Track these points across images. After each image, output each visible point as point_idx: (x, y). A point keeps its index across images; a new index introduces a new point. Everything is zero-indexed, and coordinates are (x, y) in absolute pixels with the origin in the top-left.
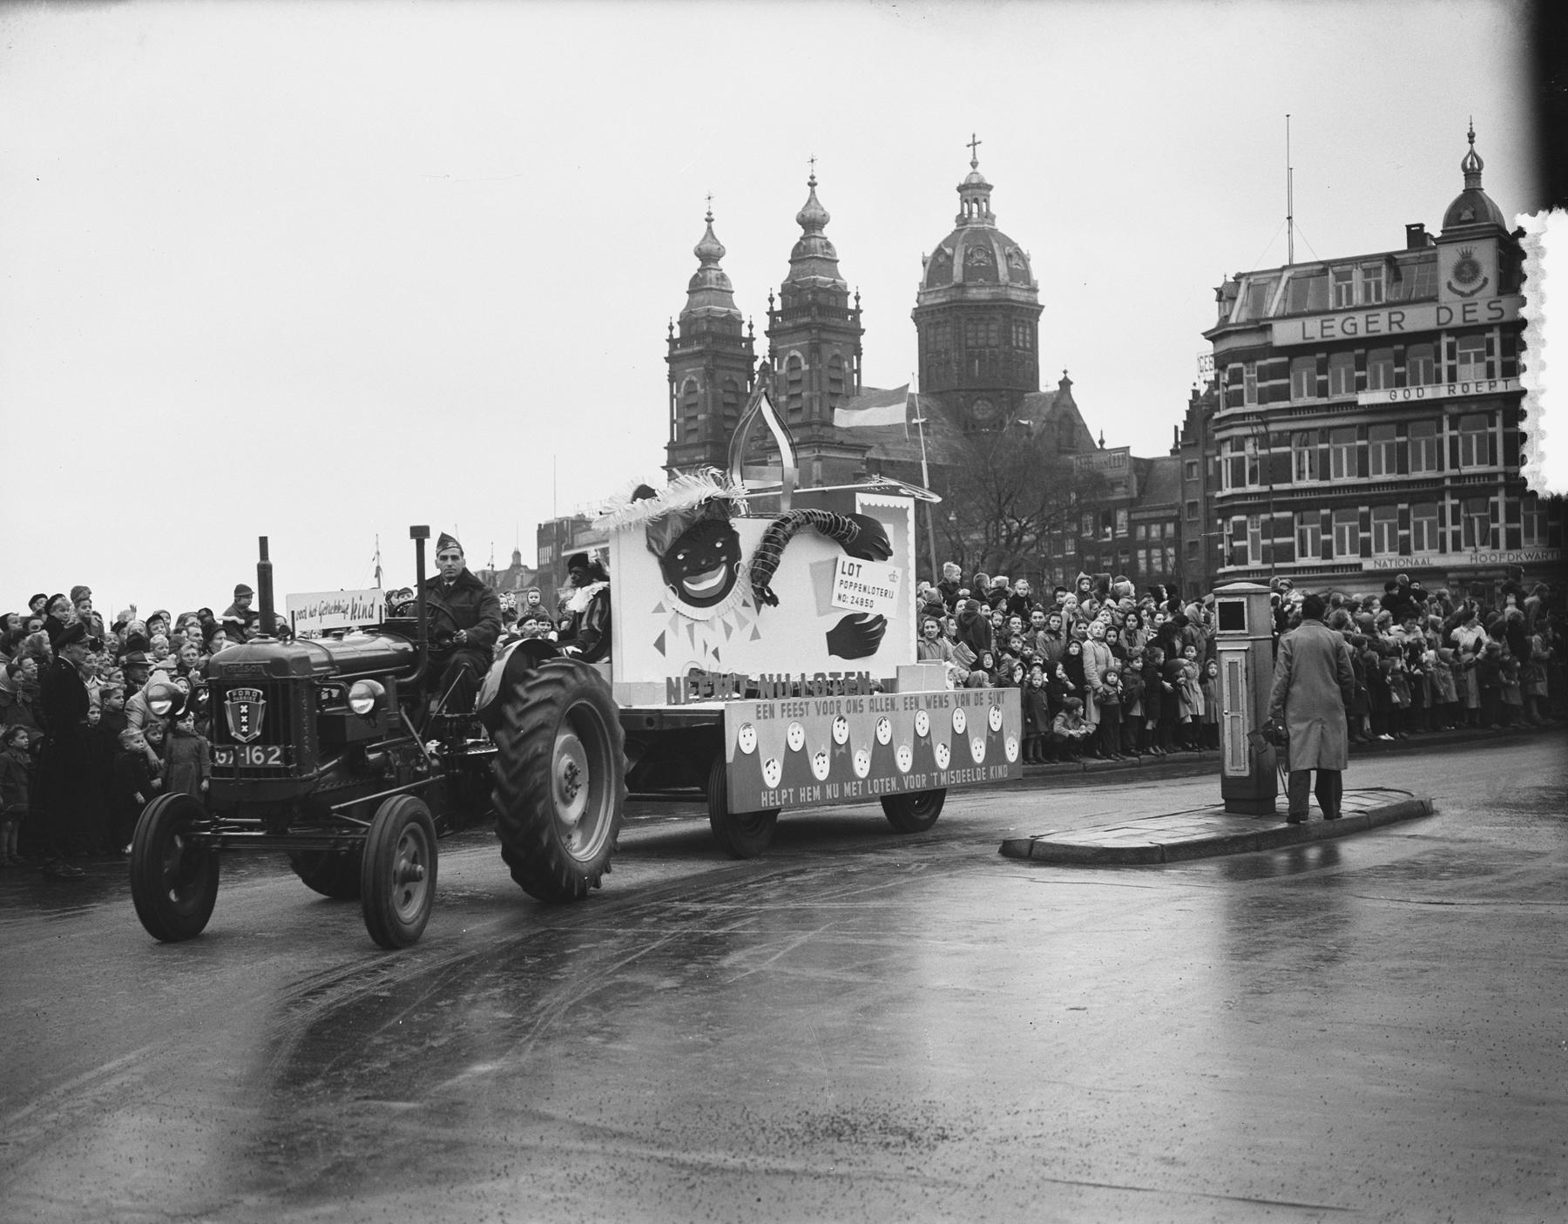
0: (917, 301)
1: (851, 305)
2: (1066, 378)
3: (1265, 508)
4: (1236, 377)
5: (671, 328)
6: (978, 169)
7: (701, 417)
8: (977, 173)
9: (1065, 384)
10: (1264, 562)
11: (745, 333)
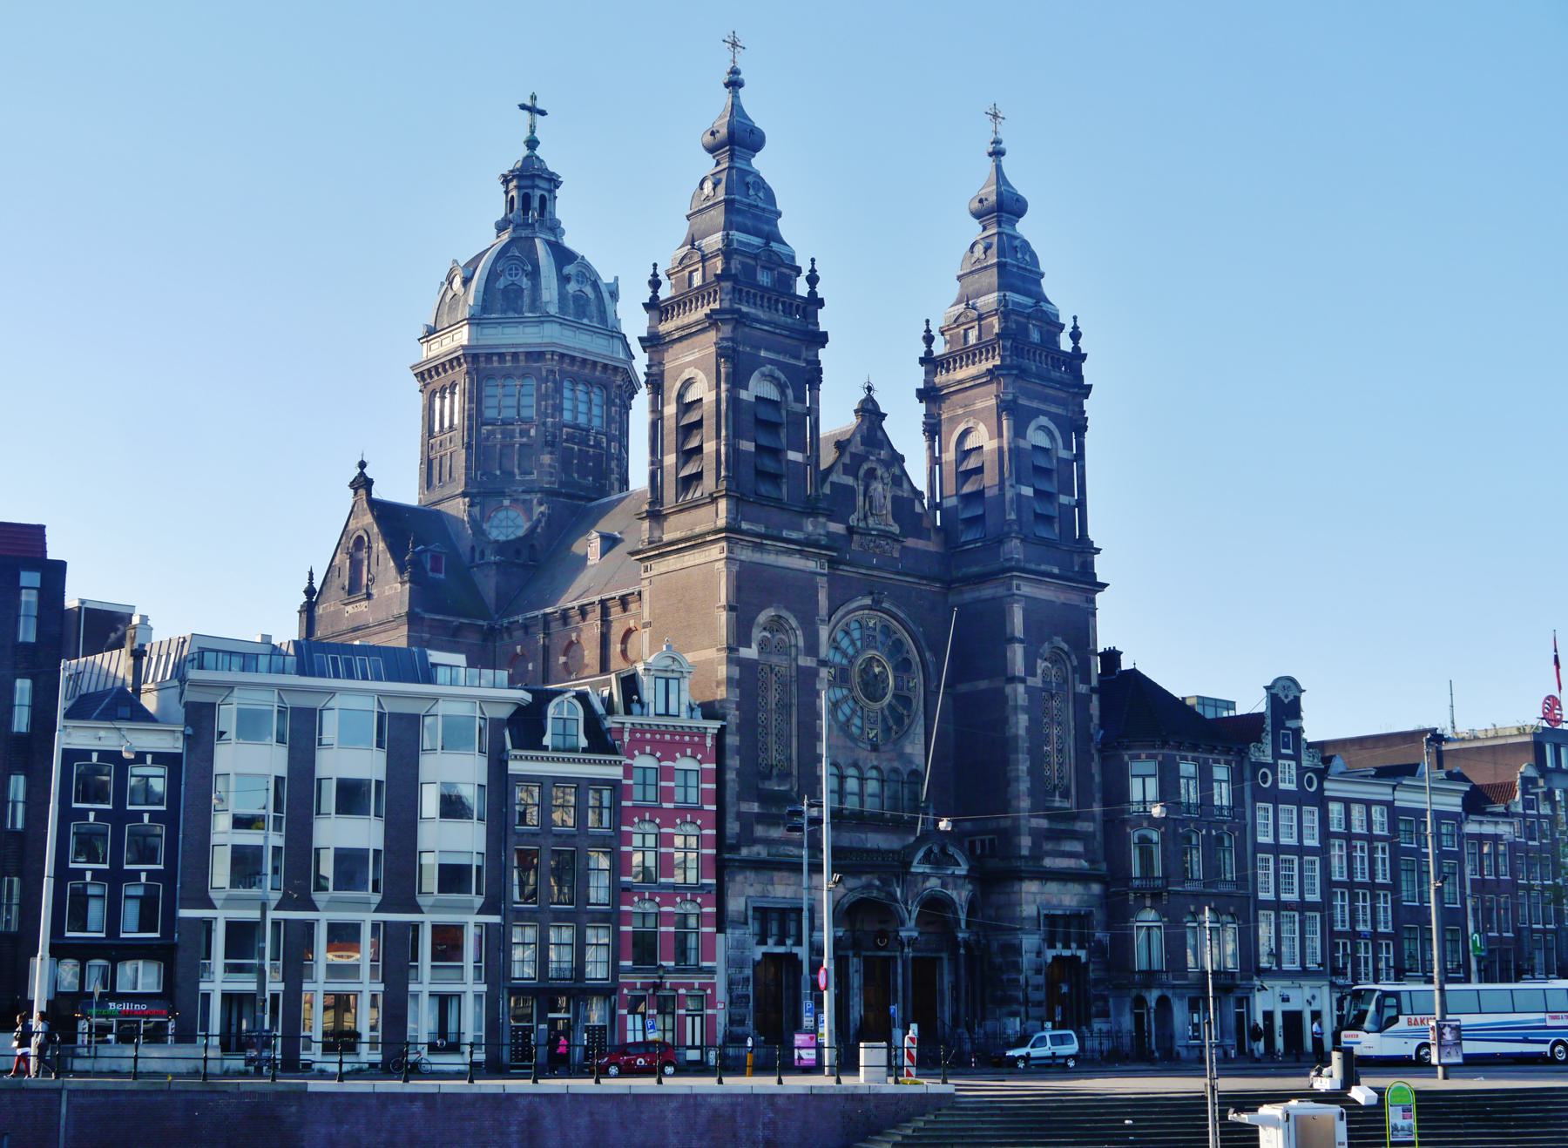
6: (538, 152)
7: (709, 447)
8: (537, 158)
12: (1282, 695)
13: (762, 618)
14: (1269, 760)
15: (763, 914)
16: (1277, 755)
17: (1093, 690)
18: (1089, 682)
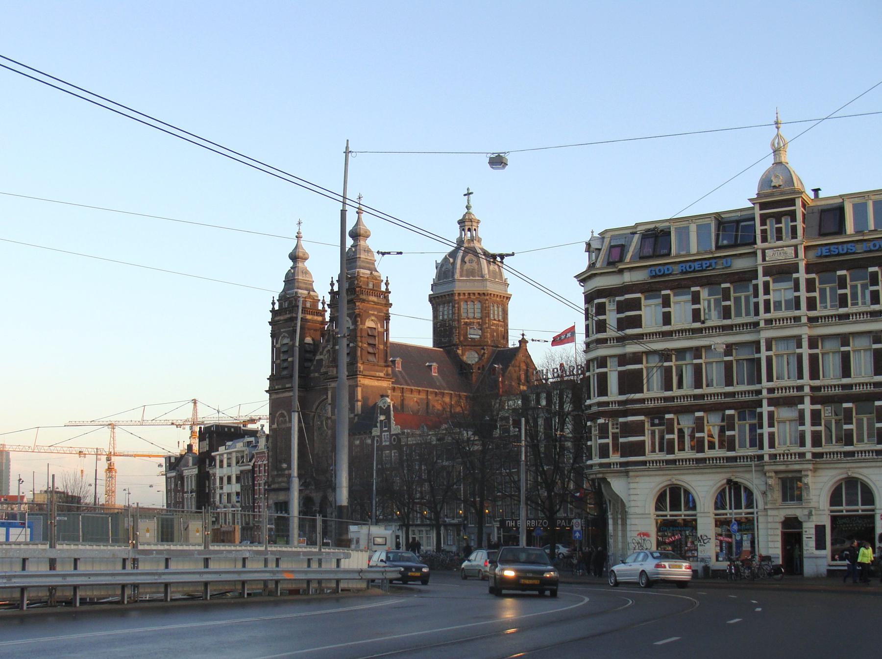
0: (432, 290)
1: (383, 288)
2: (523, 338)
3: (625, 413)
4: (601, 310)
5: (273, 304)
6: (470, 211)
8: (470, 214)
9: (523, 342)
10: (622, 456)
11: (320, 307)
12: (382, 406)
13: (277, 415)
14: (379, 434)
15: (276, 504)
16: (382, 432)
17: (355, 415)
18: (354, 412)
